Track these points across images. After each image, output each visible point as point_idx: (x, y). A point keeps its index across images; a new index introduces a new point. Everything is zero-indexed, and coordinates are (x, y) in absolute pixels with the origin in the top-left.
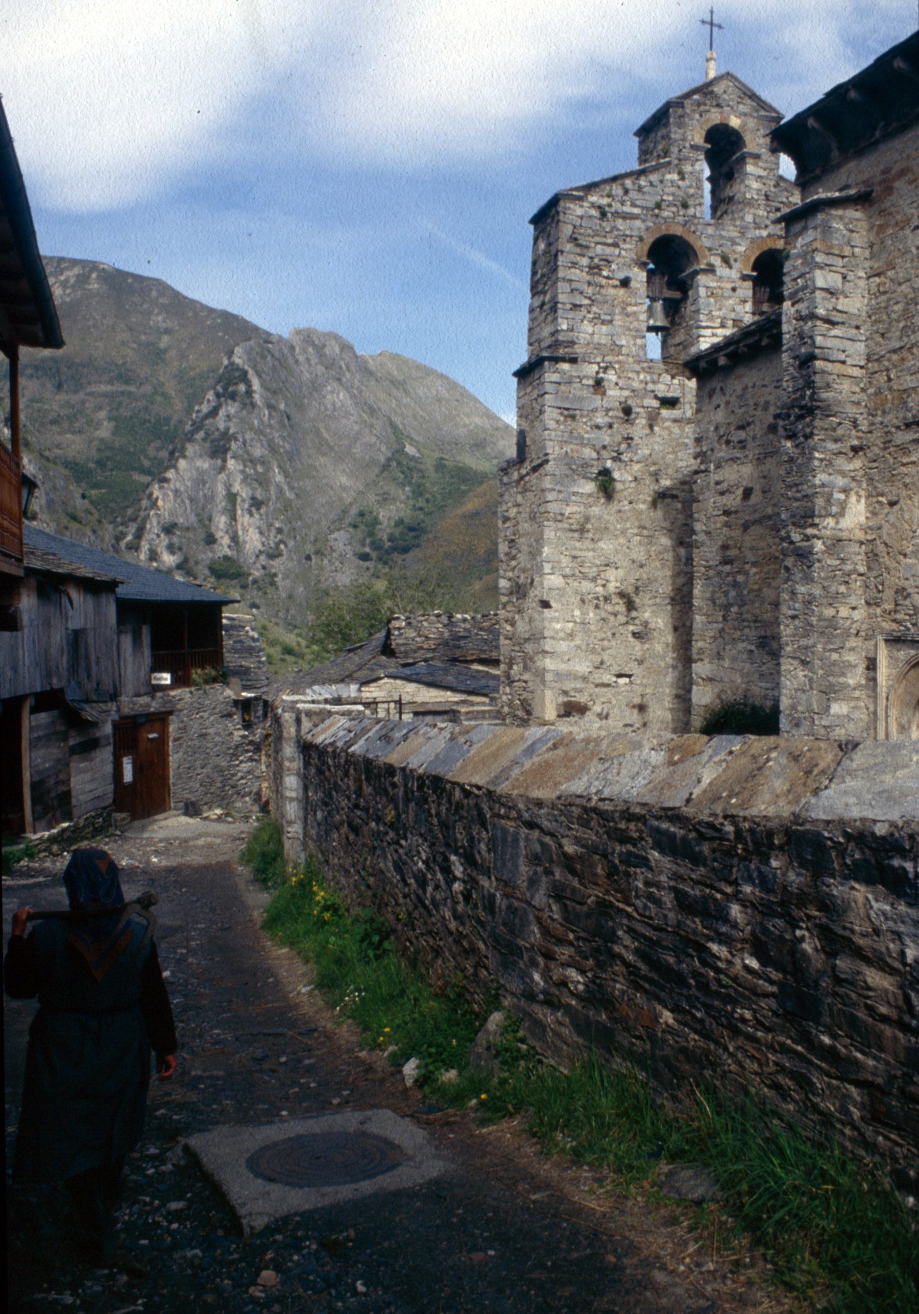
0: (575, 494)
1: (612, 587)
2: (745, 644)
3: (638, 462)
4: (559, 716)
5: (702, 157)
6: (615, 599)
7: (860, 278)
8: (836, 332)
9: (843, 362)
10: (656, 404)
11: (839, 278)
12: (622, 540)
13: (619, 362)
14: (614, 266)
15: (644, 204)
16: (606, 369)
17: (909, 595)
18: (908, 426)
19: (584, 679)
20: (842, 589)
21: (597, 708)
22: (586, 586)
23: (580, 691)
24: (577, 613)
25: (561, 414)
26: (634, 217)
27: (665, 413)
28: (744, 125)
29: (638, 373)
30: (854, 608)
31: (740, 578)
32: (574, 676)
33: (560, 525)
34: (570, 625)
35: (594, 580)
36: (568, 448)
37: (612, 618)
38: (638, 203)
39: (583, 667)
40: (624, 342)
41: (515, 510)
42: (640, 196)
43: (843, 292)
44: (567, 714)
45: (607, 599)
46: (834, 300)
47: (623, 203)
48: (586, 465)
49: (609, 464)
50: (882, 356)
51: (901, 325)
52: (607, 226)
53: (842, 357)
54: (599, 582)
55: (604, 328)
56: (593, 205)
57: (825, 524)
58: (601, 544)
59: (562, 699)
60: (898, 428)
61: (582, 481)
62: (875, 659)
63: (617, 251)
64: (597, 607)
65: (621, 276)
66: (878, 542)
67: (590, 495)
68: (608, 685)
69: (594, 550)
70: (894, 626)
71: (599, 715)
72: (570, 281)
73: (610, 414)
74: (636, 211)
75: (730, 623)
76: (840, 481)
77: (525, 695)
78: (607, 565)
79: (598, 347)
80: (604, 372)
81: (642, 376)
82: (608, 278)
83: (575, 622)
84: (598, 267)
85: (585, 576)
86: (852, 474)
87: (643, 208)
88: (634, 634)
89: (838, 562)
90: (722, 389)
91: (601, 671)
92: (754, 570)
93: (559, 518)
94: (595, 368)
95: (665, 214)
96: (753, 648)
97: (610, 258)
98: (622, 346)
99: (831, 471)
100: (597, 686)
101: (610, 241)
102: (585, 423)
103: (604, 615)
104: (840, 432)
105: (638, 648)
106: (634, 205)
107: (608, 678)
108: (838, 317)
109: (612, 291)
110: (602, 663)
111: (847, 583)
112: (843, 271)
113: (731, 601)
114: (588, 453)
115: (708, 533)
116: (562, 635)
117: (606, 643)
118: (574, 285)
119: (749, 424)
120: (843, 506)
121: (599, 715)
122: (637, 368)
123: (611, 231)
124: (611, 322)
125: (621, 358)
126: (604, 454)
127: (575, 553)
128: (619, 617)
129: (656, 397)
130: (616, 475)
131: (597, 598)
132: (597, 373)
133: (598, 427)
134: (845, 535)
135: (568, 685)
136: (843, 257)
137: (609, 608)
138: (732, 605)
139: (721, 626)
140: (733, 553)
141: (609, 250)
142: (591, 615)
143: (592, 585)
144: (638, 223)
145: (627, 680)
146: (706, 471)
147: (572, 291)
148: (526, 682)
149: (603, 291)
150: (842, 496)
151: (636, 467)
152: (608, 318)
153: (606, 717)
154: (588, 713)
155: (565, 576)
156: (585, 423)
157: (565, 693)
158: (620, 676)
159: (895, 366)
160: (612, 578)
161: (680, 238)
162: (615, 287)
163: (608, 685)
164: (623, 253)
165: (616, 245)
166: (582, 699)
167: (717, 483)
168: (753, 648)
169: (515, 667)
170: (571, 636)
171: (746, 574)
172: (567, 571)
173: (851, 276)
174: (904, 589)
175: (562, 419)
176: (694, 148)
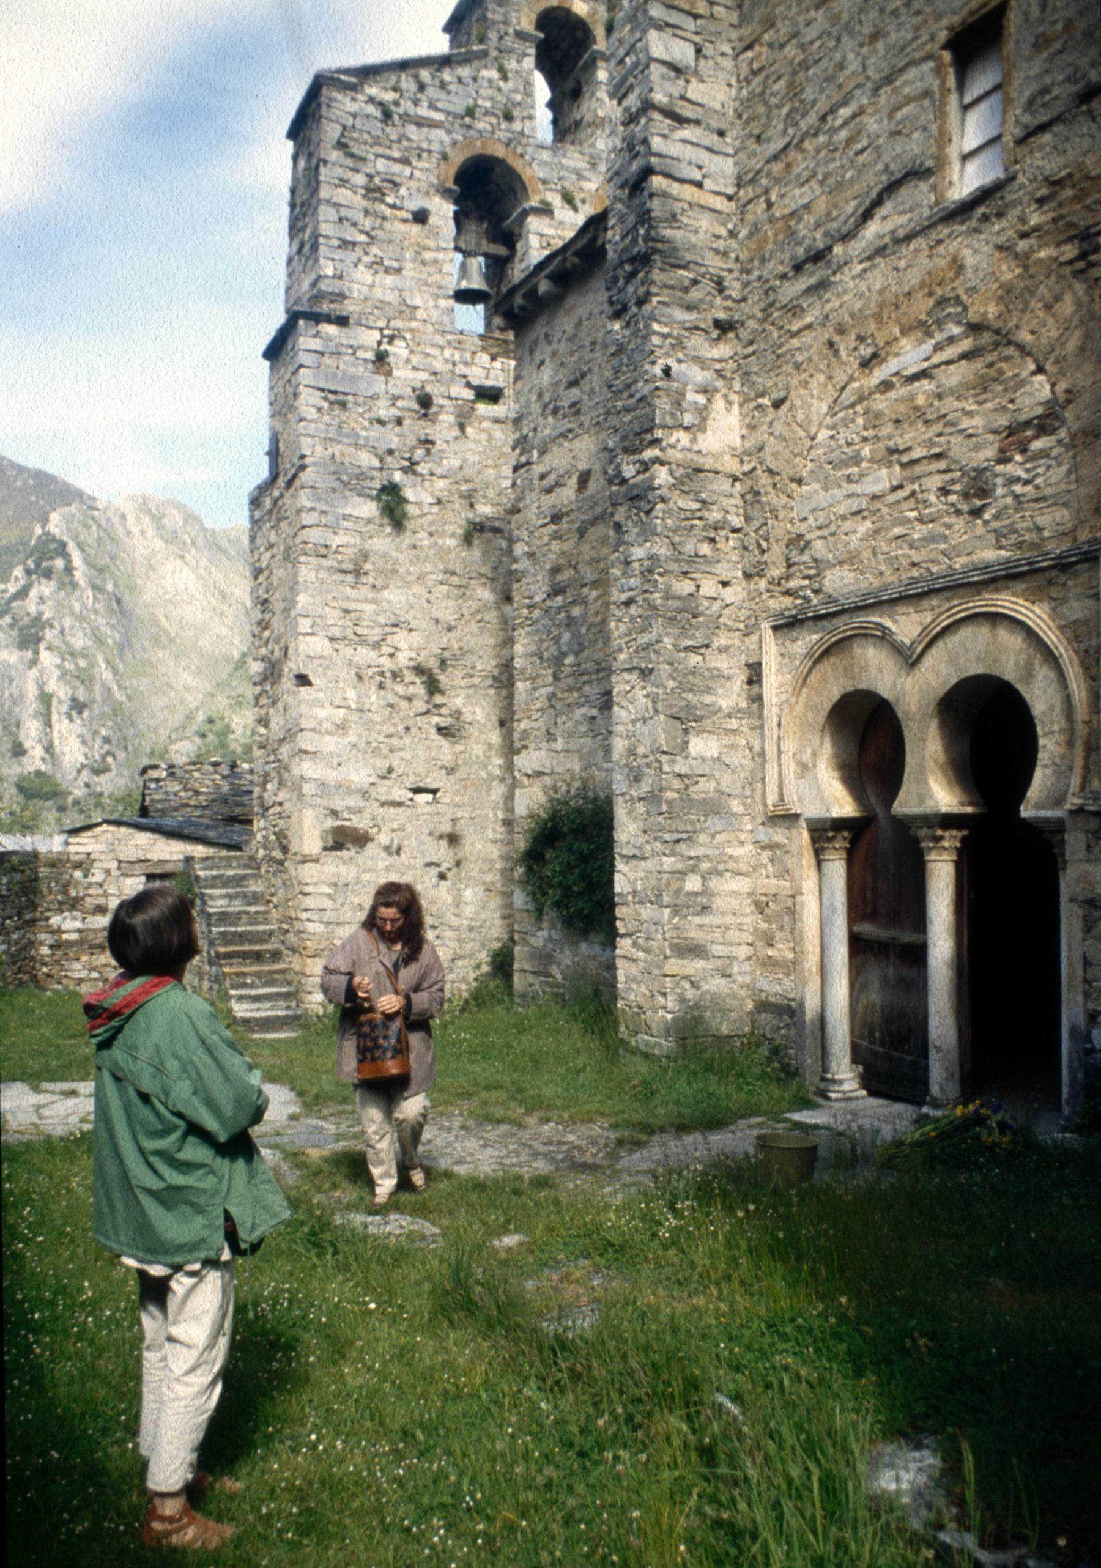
0: (345, 517)
1: (403, 659)
2: (583, 710)
3: (443, 477)
4: (325, 849)
5: (532, 51)
6: (409, 676)
7: (723, 54)
8: (687, 133)
9: (699, 185)
10: (470, 395)
11: (690, 51)
12: (417, 589)
13: (412, 330)
14: (403, 191)
15: (451, 108)
16: (391, 339)
17: (808, 544)
18: (798, 268)
19: (365, 794)
20: (705, 549)
21: (383, 839)
22: (365, 655)
25: (325, 399)
26: (433, 125)
27: (482, 408)
28: (593, 13)
29: (442, 348)
30: (725, 584)
31: (576, 611)
32: (345, 788)
33: (324, 562)
34: (342, 711)
35: (376, 646)
36: (337, 449)
37: (404, 704)
38: (439, 105)
39: (360, 775)
40: (418, 302)
41: (268, 555)
42: (442, 95)
43: (696, 72)
44: (338, 846)
45: (395, 675)
46: (681, 82)
47: (416, 102)
48: (362, 476)
49: (398, 477)
50: (758, 172)
51: (785, 111)
52: (393, 133)
53: (697, 175)
54: (386, 650)
55: (389, 280)
56: (371, 100)
57: (673, 440)
58: (386, 594)
59: (330, 823)
60: (784, 277)
61: (357, 499)
62: (760, 664)
63: (407, 171)
64: (381, 686)
65: (414, 205)
66: (759, 472)
67: (369, 521)
68: (399, 804)
69: (375, 601)
70: (787, 601)
71: (387, 849)
72: (337, 205)
73: (399, 403)
74: (439, 116)
75: (563, 684)
76: (699, 376)
77: (282, 823)
78: (395, 625)
79: (382, 305)
80: (390, 343)
81: (447, 353)
82: (393, 207)
83: (348, 708)
84: (379, 189)
85: (362, 640)
86: (718, 366)
87: (448, 113)
88: (440, 730)
89: (695, 506)
90: (547, 336)
91: (387, 782)
92: (594, 594)
93: (323, 551)
94: (377, 335)
95: (480, 125)
96: (594, 712)
97: (398, 180)
98: (416, 308)
99: (680, 355)
100: (383, 804)
101: (396, 154)
102: (361, 415)
103: (390, 698)
104: (694, 295)
105: (446, 750)
106: (432, 106)
107: (400, 793)
108: (688, 112)
109: (401, 227)
110: (390, 770)
111: (712, 540)
112: (697, 39)
113: (564, 648)
114: (366, 459)
115: (531, 555)
116: (326, 725)
117: (394, 741)
118: (344, 212)
119: (583, 375)
120: (703, 413)
121: (387, 849)
123: (399, 141)
124: (399, 271)
125: (414, 324)
126: (389, 459)
127: (346, 605)
128: (415, 703)
129: (468, 385)
130: (409, 493)
131: (382, 674)
132: (379, 343)
133: (381, 422)
134: (708, 463)
135: (339, 803)
136: (696, 17)
137: (400, 689)
138: (564, 654)
139: (550, 689)
140: (567, 575)
141: (396, 168)
142: (373, 698)
143: (373, 654)
144: (440, 134)
145: (430, 797)
146: (528, 463)
147: (341, 220)
148: (281, 804)
149: (387, 225)
150: (701, 399)
151: (441, 484)
152: (395, 264)
153: (398, 852)
154: (370, 845)
155: (332, 639)
156: (361, 415)
157: (334, 813)
158: (417, 790)
159: (777, 181)
160: (403, 645)
161: (501, 162)
162: (405, 221)
163: (399, 804)
164: (417, 173)
165: (406, 161)
166: (360, 823)
167: (543, 477)
168: (594, 712)
169: (269, 786)
170: (342, 728)
171: (584, 602)
172: (337, 632)
173: (708, 49)
174: (800, 536)
175: (326, 405)
176: (520, 35)
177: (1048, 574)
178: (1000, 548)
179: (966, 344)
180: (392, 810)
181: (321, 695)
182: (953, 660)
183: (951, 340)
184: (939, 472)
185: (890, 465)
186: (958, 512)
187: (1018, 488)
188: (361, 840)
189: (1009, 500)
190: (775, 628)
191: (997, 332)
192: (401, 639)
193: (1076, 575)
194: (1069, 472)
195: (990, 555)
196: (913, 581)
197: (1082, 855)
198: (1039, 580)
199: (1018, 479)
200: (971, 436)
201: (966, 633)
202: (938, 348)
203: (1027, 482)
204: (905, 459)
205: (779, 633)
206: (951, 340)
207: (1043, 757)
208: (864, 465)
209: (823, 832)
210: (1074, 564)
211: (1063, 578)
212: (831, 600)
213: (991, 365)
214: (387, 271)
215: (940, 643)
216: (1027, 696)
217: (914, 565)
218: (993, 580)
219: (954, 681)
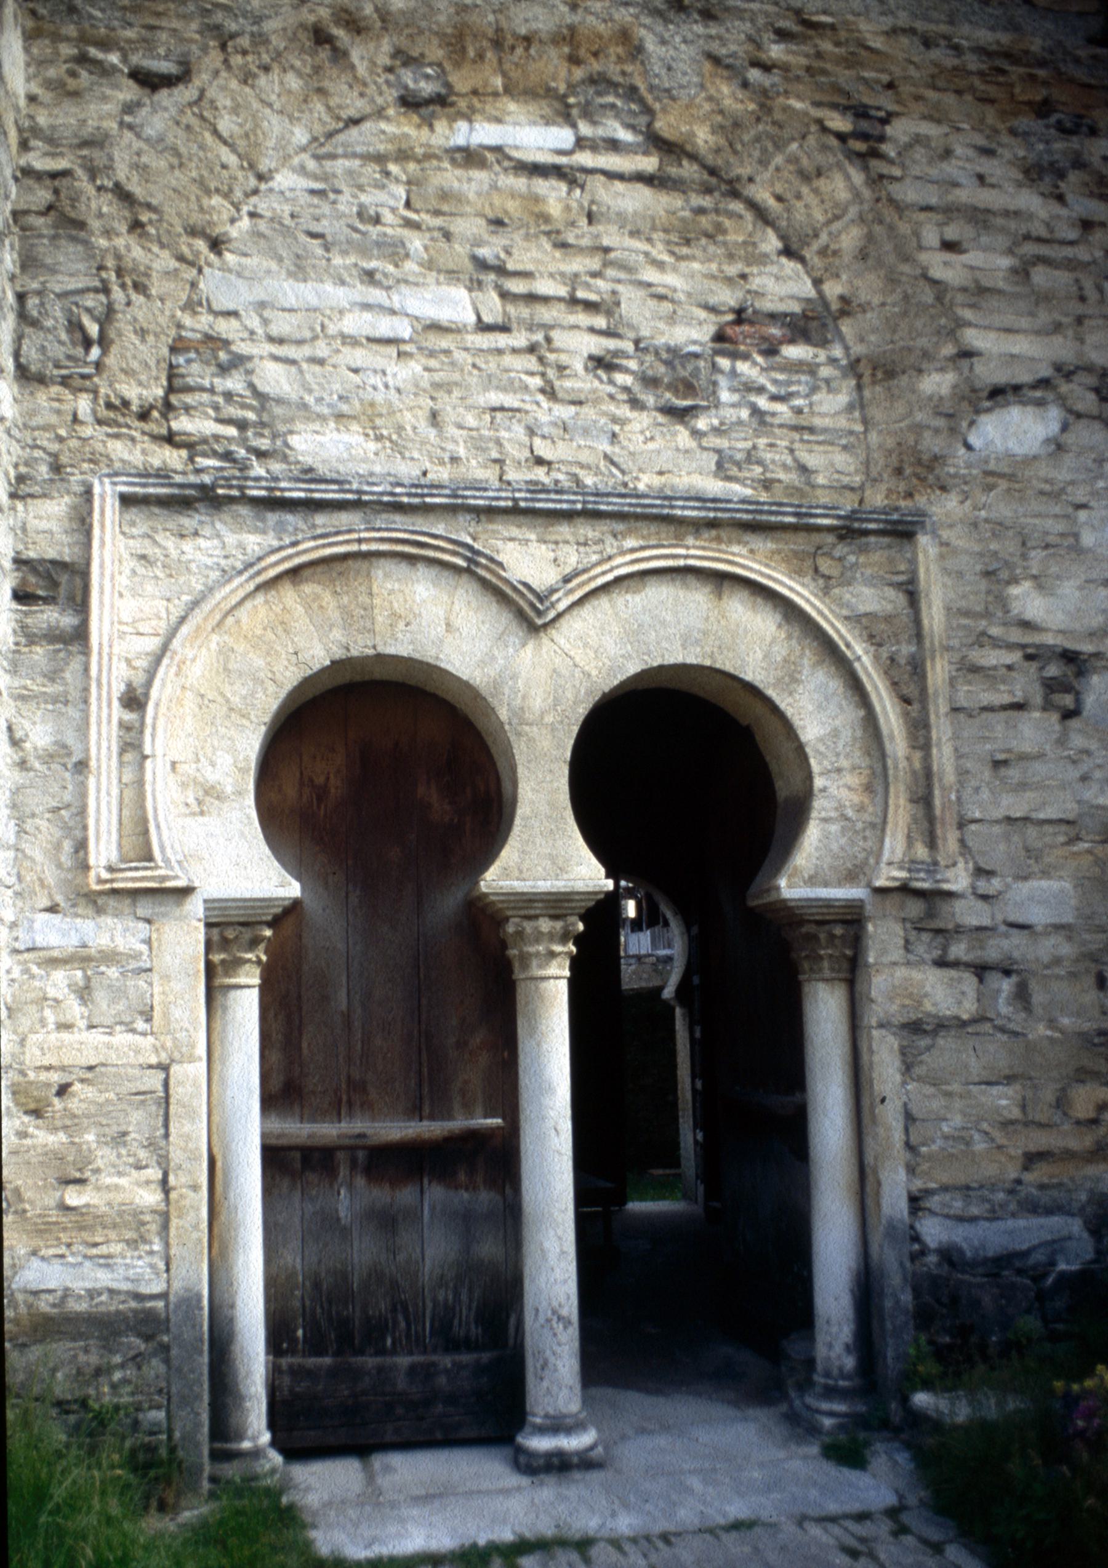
70: (174, 458)
177: (816, 538)
178: (729, 479)
179: (649, 163)
182: (634, 634)
183: (614, 145)
184: (592, 330)
185: (475, 285)
186: (635, 404)
187: (762, 402)
189: (745, 414)
190: (127, 501)
191: (713, 172)
193: (864, 550)
194: (850, 408)
195: (714, 487)
196: (536, 488)
197: (897, 954)
198: (800, 542)
199: (761, 390)
200: (661, 298)
201: (658, 593)
202: (581, 143)
203: (774, 398)
204: (517, 286)
205: (133, 513)
206: (614, 145)
207: (820, 806)
208: (410, 266)
209: (229, 929)
210: (866, 533)
211: (840, 550)
212: (309, 475)
213: (701, 211)
215: (603, 602)
216: (789, 712)
217: (540, 461)
218: (713, 524)
219: (633, 668)
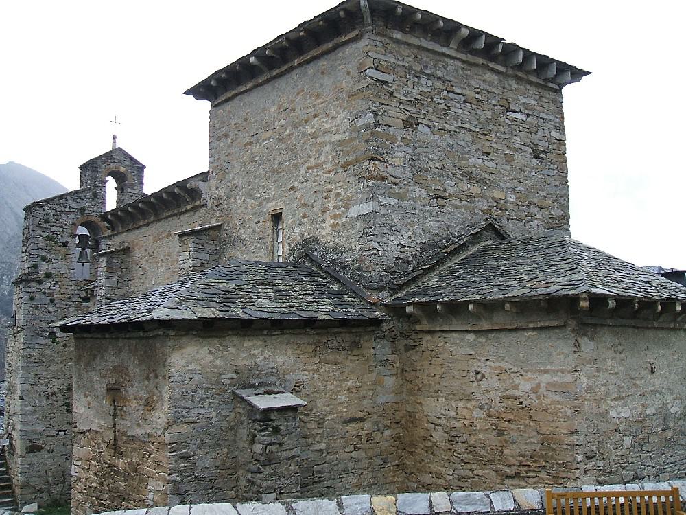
1: (55, 388)
19: (41, 434)
22: (43, 388)
23: (39, 440)
24: (37, 402)
26: (71, 213)
28: (127, 170)
32: (35, 432)
35: (47, 385)
38: (73, 207)
39: (40, 428)
45: (52, 394)
59: (28, 444)
69: (47, 371)
71: (49, 451)
81: (73, 288)
95: (87, 212)
101: (59, 225)
107: (53, 432)
121: (49, 451)
122: (70, 283)
129: (80, 297)
131: (48, 394)
137: (55, 398)
141: (57, 229)
152: (56, 261)
157: (30, 441)
158: (59, 431)
160: (56, 384)
165: (61, 227)
166: (39, 443)
170: (34, 413)
172: (33, 382)
173: (121, 280)
180: (50, 438)
181: (27, 403)
188: (39, 449)
192: (55, 382)
214: (54, 263)
